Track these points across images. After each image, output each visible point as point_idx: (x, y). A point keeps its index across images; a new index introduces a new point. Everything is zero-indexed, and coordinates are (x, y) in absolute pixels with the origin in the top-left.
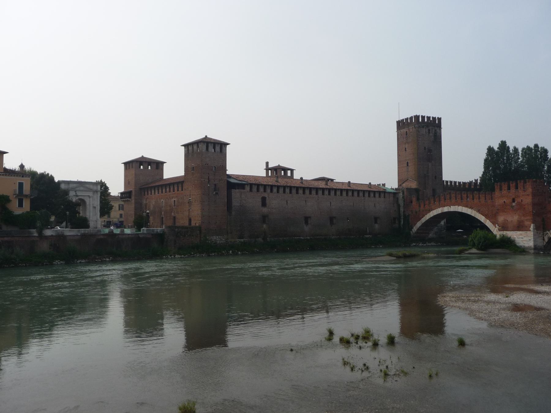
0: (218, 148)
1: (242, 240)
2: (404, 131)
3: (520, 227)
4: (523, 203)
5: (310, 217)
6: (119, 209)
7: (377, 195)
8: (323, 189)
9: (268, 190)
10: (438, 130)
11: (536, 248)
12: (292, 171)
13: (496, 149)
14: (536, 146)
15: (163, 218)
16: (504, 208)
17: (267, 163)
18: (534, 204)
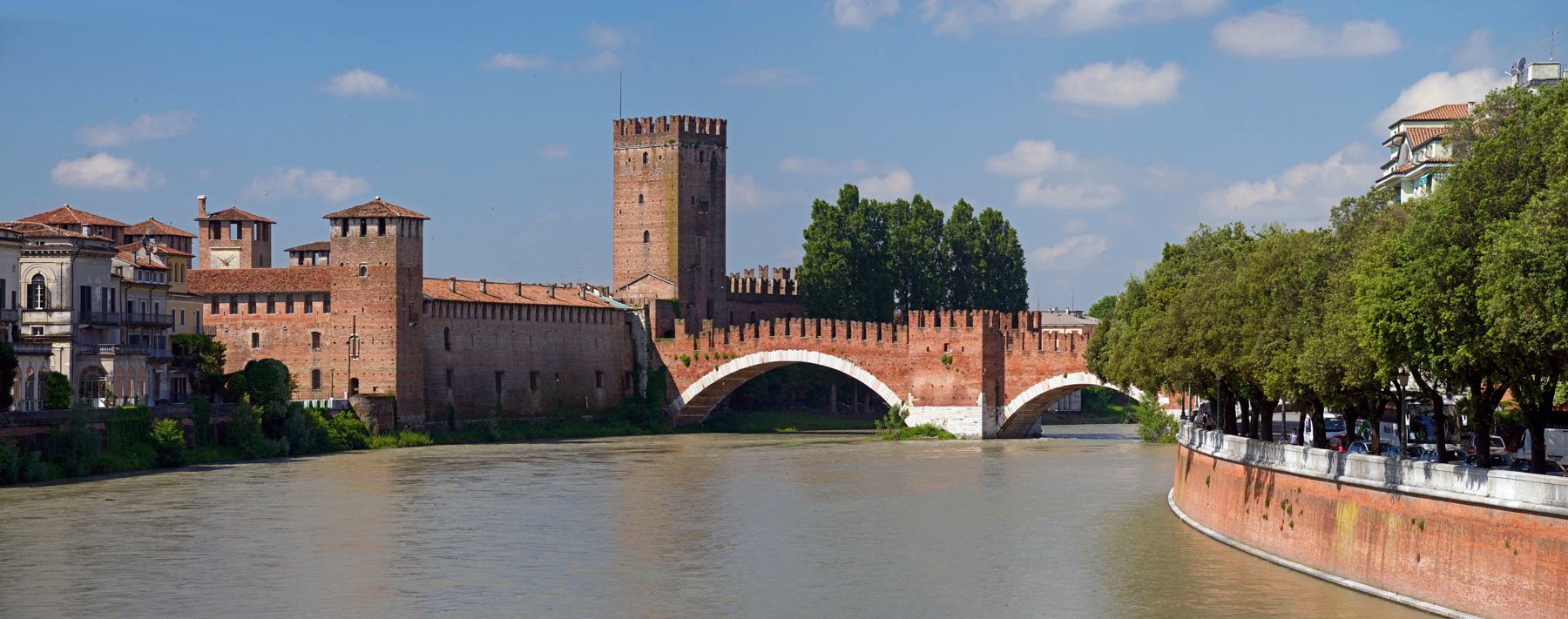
3: (957, 398)
10: (719, 153)
16: (926, 360)
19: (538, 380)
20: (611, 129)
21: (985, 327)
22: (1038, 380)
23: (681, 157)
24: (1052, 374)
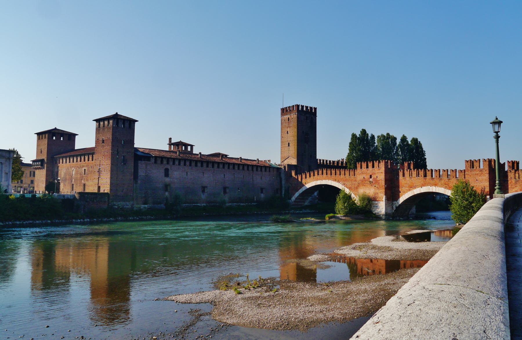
0: (127, 124)
1: (146, 206)
2: (286, 117)
4: (378, 179)
5: (206, 187)
6: (30, 176)
7: (263, 169)
8: (219, 163)
9: (171, 163)
11: (386, 214)
12: (192, 146)
13: (358, 136)
14: (388, 134)
15: (73, 185)
16: (363, 183)
17: (170, 139)
18: (386, 180)
19: (227, 191)
20: (280, 112)
21: (386, 167)
22: (410, 190)
23: (298, 118)
24: (415, 187)
